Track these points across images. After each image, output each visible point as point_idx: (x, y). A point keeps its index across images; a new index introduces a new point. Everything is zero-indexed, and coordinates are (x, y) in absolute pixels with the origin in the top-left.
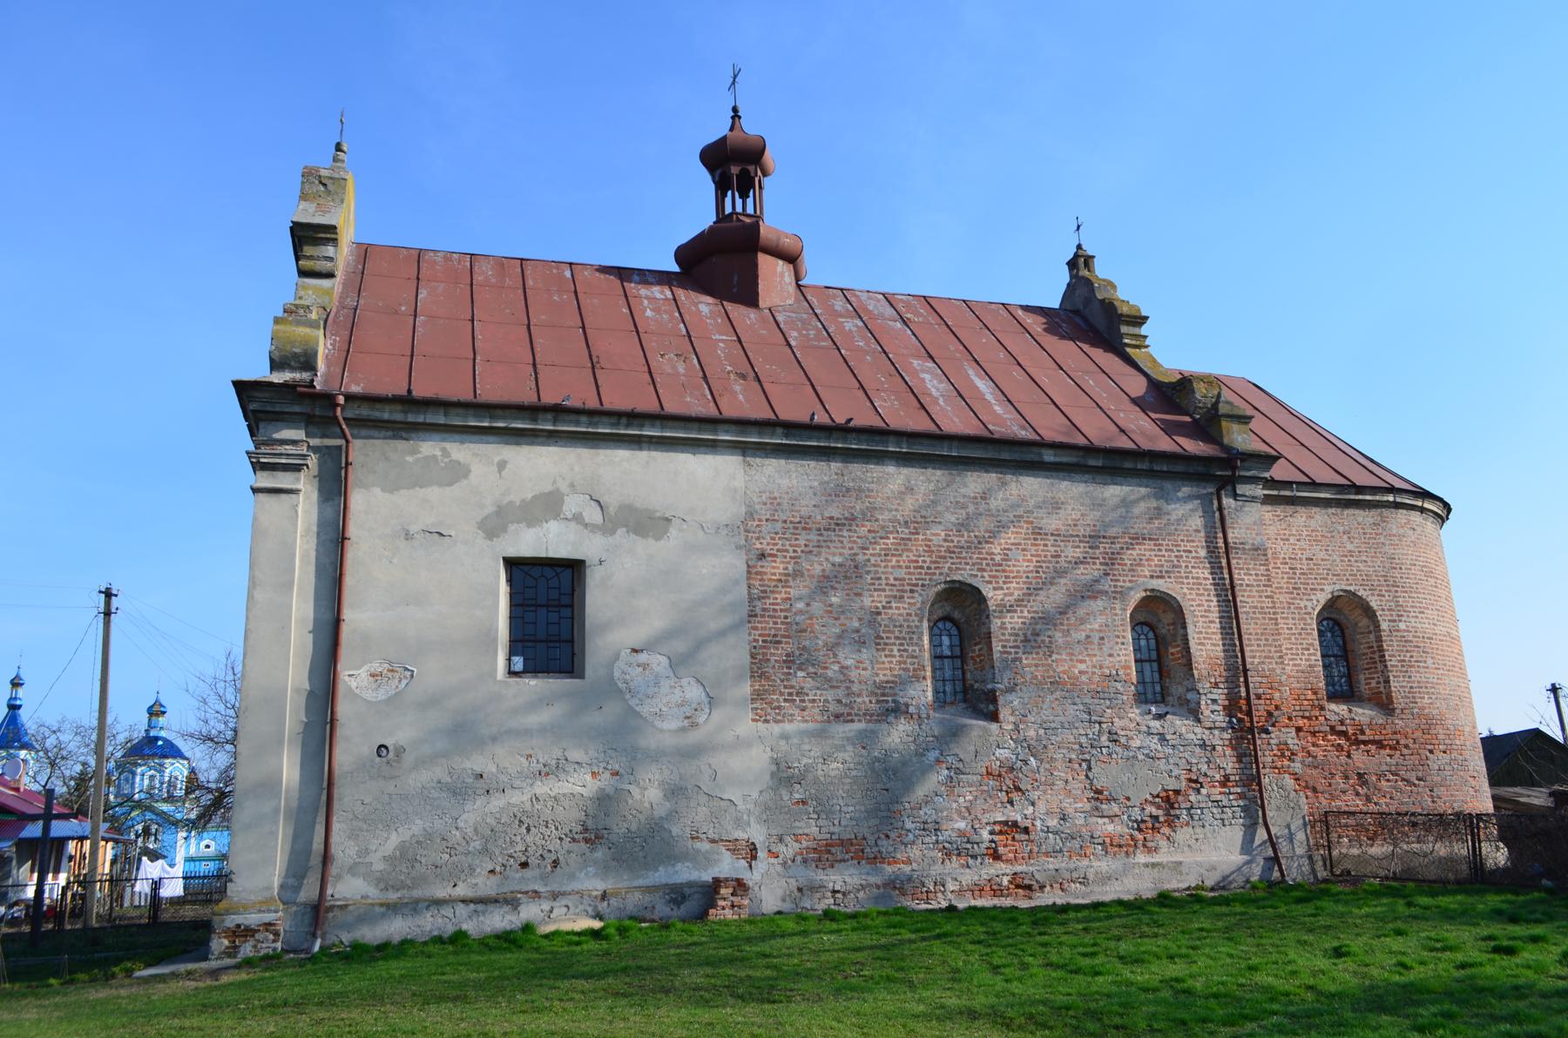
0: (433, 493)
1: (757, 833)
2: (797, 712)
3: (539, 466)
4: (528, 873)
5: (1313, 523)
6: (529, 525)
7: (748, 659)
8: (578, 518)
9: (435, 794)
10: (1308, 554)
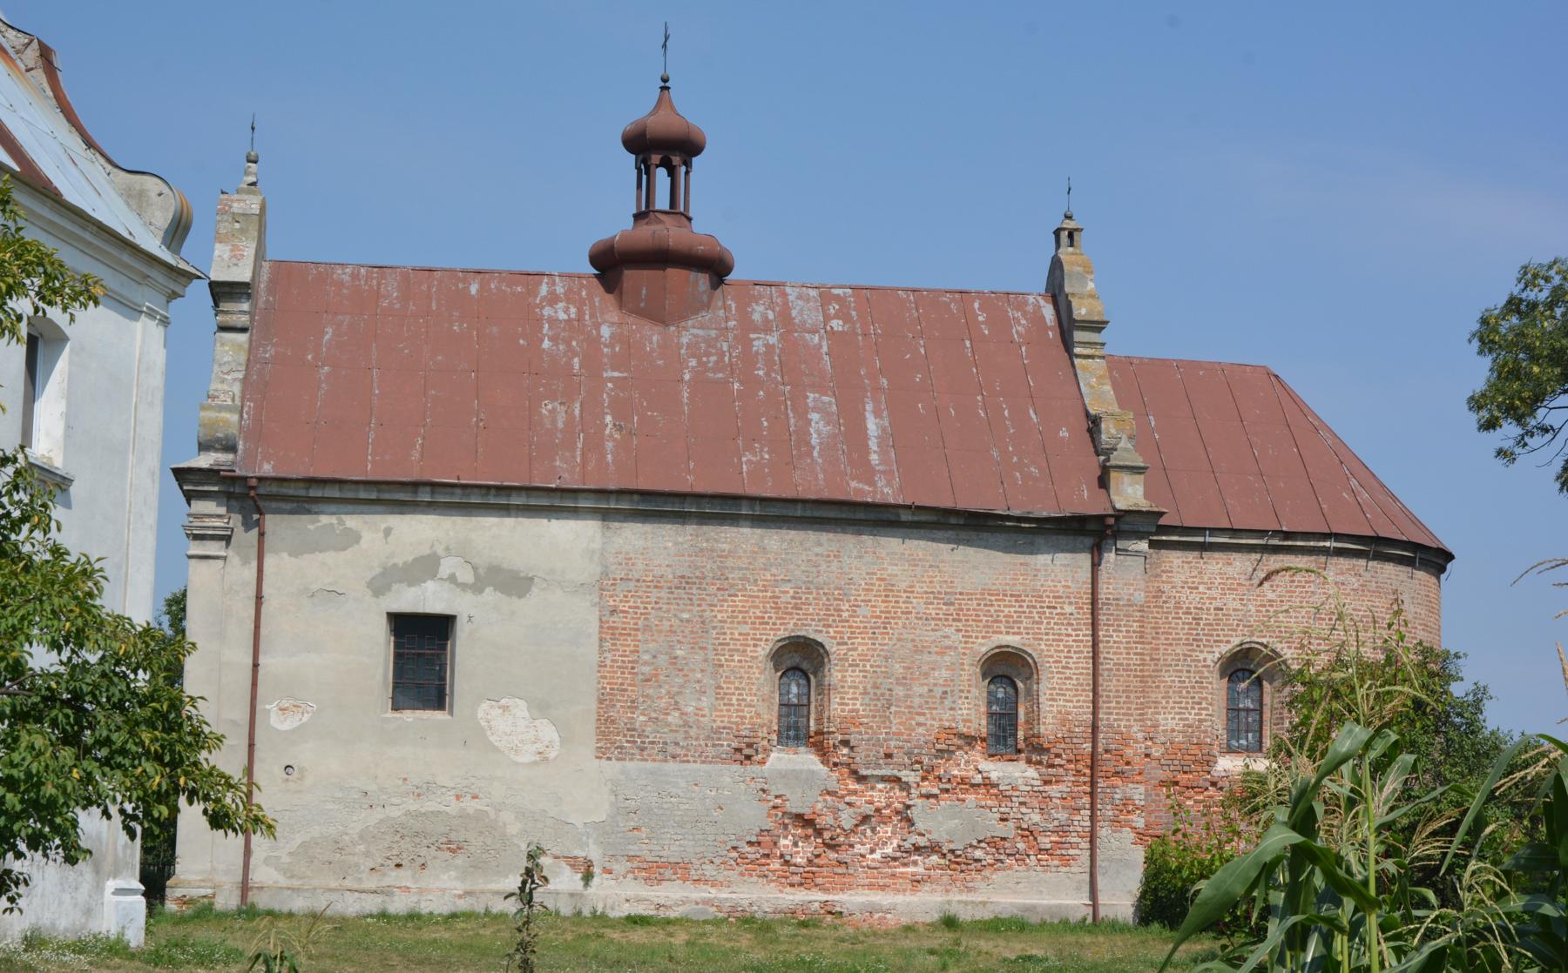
0: (329, 557)
1: (594, 853)
2: (636, 751)
3: (418, 531)
4: (400, 872)
5: (1230, 570)
6: (410, 585)
7: (594, 706)
8: (452, 578)
9: (330, 806)
10: (1218, 604)
